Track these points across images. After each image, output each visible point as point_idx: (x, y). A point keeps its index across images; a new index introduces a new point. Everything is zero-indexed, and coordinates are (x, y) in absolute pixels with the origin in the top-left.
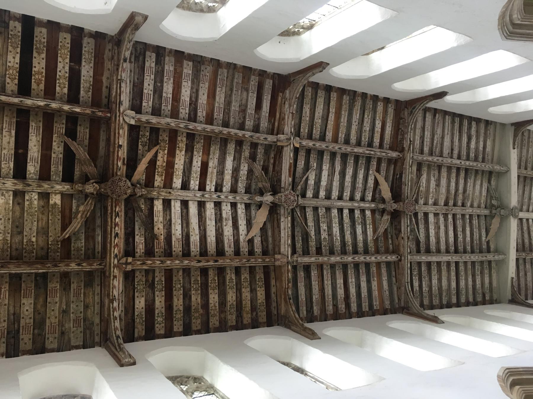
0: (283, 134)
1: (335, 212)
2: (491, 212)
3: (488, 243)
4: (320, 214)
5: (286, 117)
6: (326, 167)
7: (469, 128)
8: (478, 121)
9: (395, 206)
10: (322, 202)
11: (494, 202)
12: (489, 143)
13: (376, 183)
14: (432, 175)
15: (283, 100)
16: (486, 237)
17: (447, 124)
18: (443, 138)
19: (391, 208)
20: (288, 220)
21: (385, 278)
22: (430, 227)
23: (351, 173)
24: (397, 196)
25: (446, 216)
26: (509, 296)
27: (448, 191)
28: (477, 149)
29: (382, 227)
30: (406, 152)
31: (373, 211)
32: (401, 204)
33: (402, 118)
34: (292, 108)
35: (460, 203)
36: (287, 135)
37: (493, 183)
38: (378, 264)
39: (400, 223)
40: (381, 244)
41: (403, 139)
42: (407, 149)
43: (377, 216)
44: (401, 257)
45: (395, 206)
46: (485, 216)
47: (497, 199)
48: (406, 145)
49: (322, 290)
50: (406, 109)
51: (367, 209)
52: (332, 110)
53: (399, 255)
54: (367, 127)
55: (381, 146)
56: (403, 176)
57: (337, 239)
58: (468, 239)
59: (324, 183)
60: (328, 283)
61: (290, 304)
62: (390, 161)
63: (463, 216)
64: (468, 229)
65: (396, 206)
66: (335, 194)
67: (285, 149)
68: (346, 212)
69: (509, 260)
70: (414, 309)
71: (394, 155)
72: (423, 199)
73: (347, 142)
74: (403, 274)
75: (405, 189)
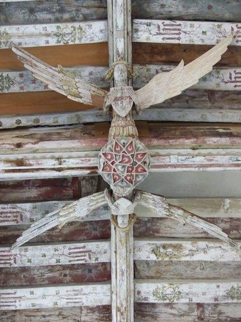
9: (124, 108)
13: (193, 51)
14: (235, 285)
19: (116, 99)
22: (63, 290)
29: (53, 76)
51: (107, 28)
72: (153, 257)
75: (183, 147)
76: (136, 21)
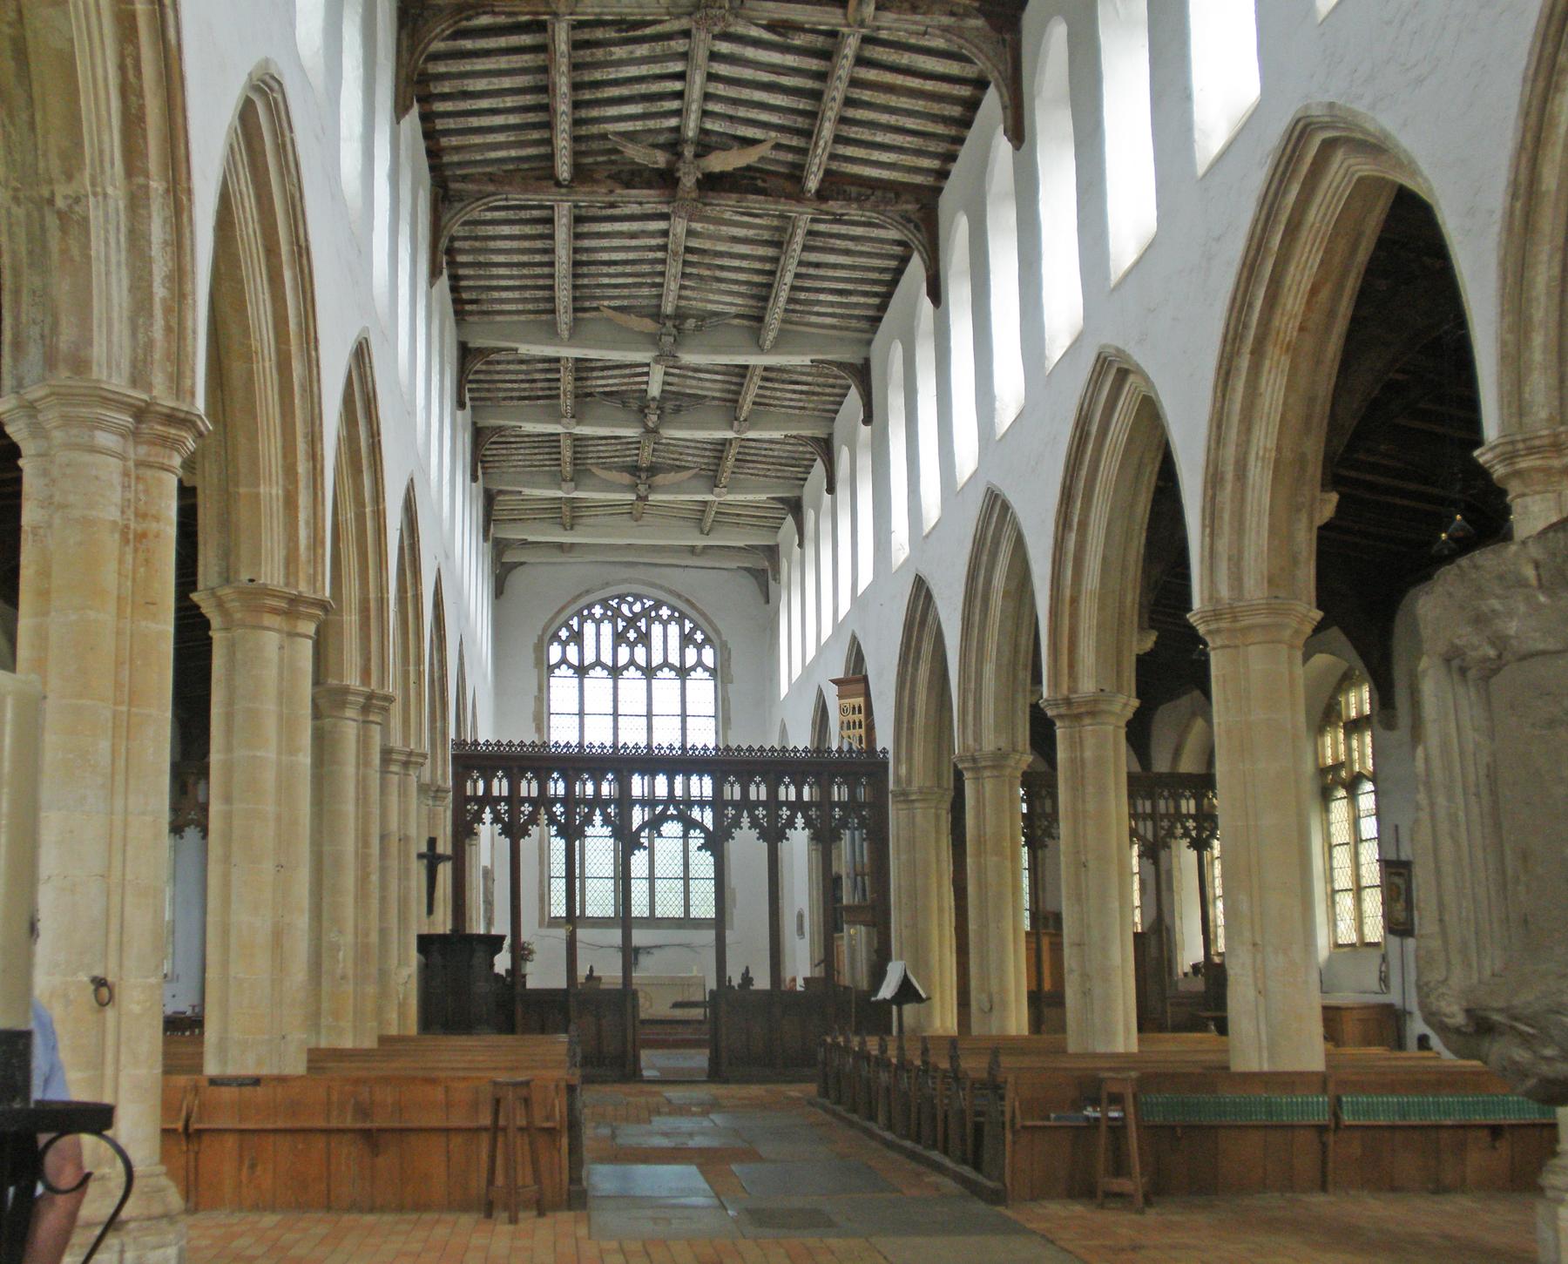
0: (878, 8)
1: (678, 67)
2: (667, 316)
3: (597, 309)
4: (673, 43)
5: (918, 18)
6: (790, 60)
7: (865, 294)
8: (883, 307)
10: (702, 44)
11: (691, 323)
12: (828, 320)
15: (961, 11)
16: (609, 307)
17: (879, 261)
18: (847, 252)
20: (661, 15)
21: (513, 153)
23: (772, 101)
24: (712, 183)
25: (664, 248)
26: (476, 342)
27: (721, 254)
28: (819, 303)
30: (816, 205)
31: (677, 129)
32: (694, 195)
33: (898, 195)
34: (937, 32)
35: (689, 270)
36: (875, 18)
37: (736, 322)
38: (549, 142)
39: (649, 185)
40: (595, 145)
41: (848, 199)
42: (824, 207)
43: (662, 139)
44: (566, 186)
45: (688, 181)
46: (659, 306)
47: (698, 328)
48: (834, 206)
49: (487, 53)
50: (918, 206)
52: (929, 86)
53: (572, 180)
54: (879, 138)
55: (833, 157)
56: (762, 198)
57: (609, 73)
58: (606, 281)
59: (750, 53)
60: (503, 63)
61: (456, 23)
62: (796, 175)
63: (662, 274)
64: (630, 280)
65: (689, 184)
66: (722, 69)
67: (839, 11)
68: (677, 86)
69: (556, 345)
70: (449, 216)
71: (813, 184)
73: (849, 102)
74: (526, 191)
75: (730, 199)
76: (705, 119)
